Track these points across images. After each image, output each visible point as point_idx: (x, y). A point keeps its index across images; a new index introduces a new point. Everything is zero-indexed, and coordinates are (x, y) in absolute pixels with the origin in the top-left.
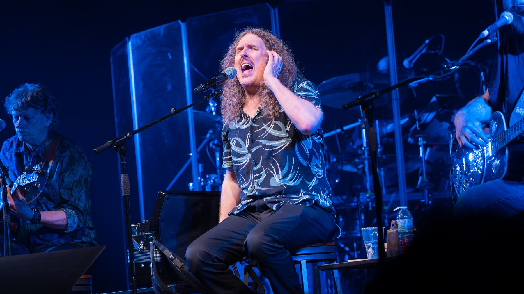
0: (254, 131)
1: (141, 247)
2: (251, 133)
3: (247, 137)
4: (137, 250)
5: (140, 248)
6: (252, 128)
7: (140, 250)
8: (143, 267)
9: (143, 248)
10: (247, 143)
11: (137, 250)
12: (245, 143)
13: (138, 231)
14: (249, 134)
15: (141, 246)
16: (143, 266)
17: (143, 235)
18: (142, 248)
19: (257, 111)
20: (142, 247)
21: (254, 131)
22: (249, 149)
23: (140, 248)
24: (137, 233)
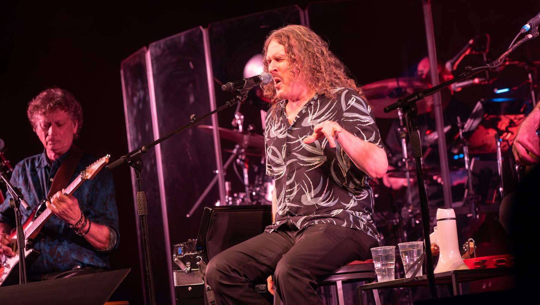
0: (290, 143)
1: (187, 269)
2: (287, 144)
3: (283, 149)
4: (184, 272)
5: (187, 270)
6: (288, 139)
7: (186, 271)
8: (192, 290)
9: (190, 269)
10: (283, 154)
11: (184, 272)
12: (282, 155)
13: (184, 251)
14: (285, 145)
15: (187, 267)
16: (190, 289)
17: (190, 255)
18: (189, 269)
19: (294, 122)
20: (189, 268)
21: (290, 143)
22: (285, 161)
23: (186, 269)
24: (182, 253)
